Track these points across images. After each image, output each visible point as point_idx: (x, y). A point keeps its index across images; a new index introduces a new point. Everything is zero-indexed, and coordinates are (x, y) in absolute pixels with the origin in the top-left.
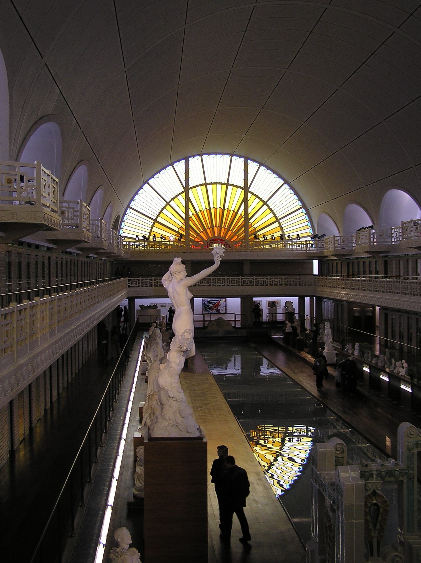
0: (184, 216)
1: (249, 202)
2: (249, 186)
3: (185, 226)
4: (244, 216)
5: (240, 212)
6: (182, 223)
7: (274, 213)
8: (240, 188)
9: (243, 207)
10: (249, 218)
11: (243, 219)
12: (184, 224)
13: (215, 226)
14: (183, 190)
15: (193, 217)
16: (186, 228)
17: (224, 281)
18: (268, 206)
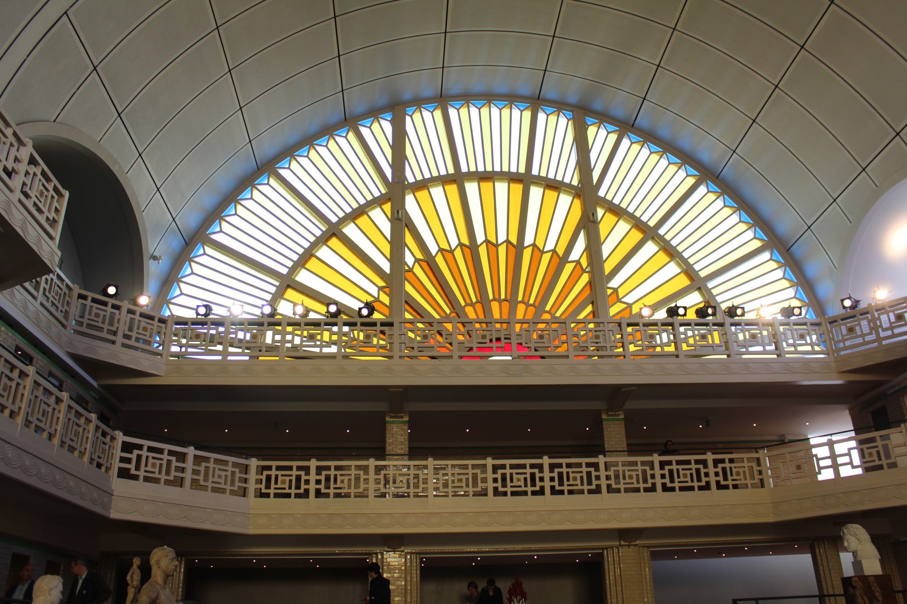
0: (386, 266)
1: (601, 226)
6: (381, 289)
9: (581, 243)
11: (585, 278)
13: (494, 300)
15: (418, 270)
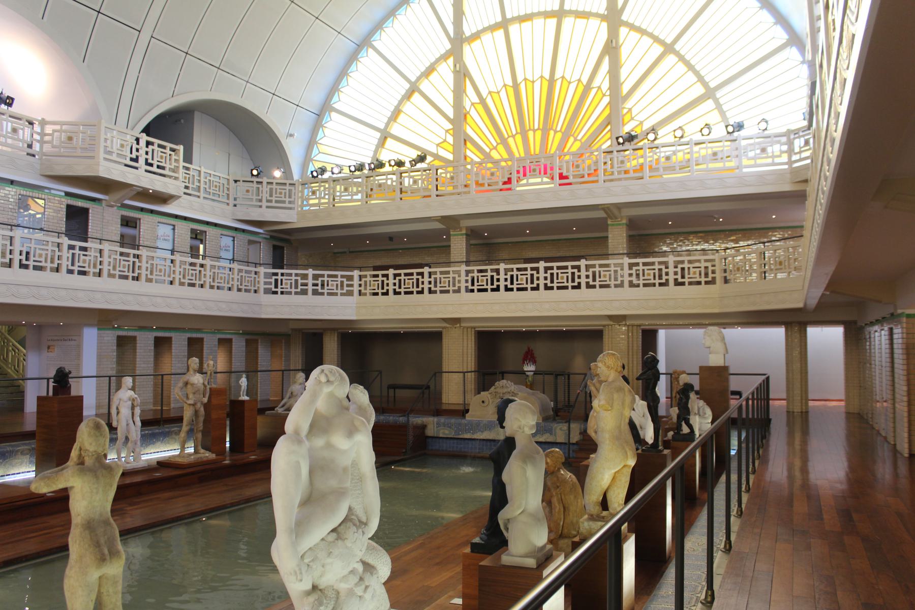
0: (450, 113)
4: (608, 93)
5: (596, 83)
8: (597, 15)
11: (606, 100)
12: (451, 132)
14: (448, 46)
16: (454, 141)
17: (536, 276)
18: (677, 54)
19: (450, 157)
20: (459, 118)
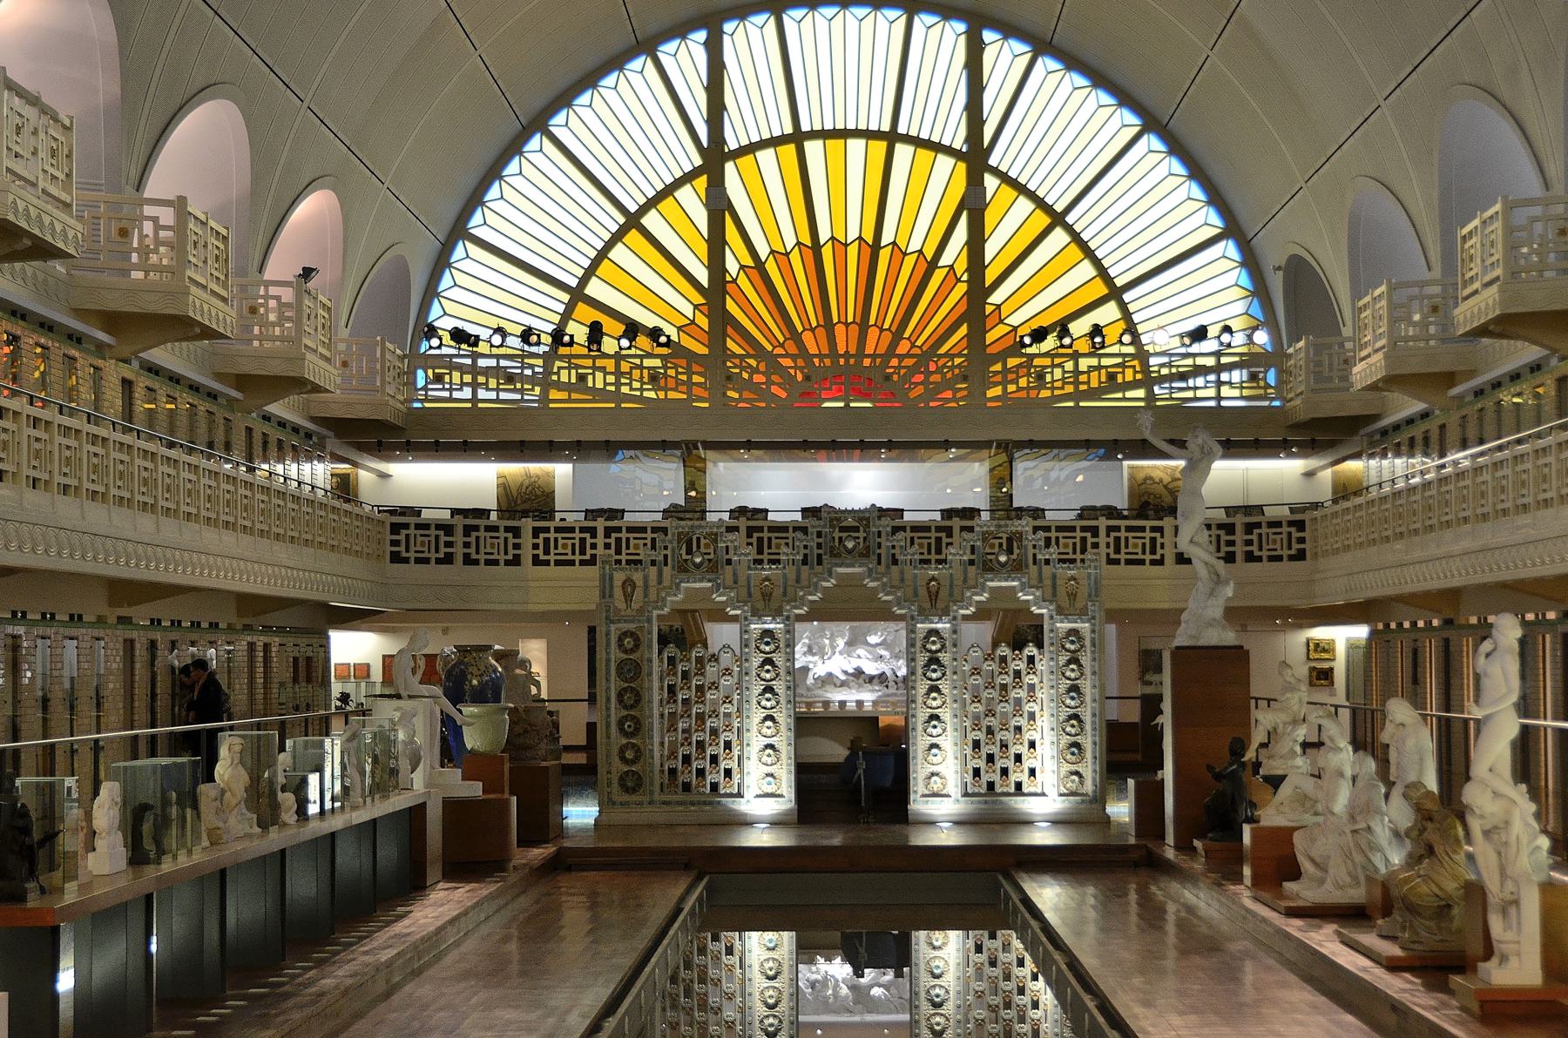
0: (702, 276)
2: (986, 144)
3: (706, 320)
4: (965, 278)
5: (946, 259)
6: (696, 307)
7: (1097, 263)
8: (949, 151)
10: (987, 284)
11: (962, 288)
12: (705, 309)
14: (698, 161)
15: (743, 281)
19: (703, 350)
20: (716, 291)
